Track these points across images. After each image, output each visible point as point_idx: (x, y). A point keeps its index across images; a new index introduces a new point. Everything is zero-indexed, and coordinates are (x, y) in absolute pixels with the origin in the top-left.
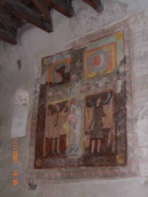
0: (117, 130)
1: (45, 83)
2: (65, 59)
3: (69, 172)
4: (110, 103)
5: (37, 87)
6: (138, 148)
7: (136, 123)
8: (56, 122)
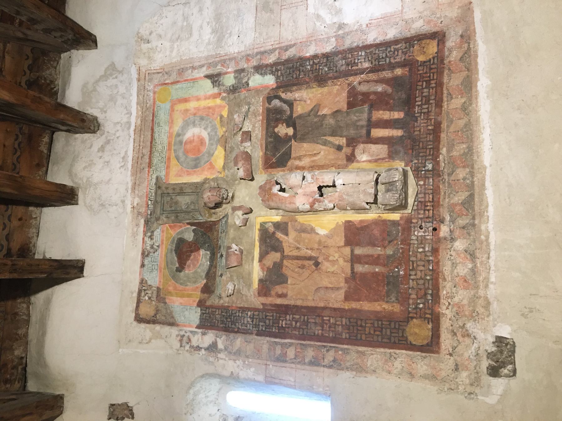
0: (357, 70)
1: (199, 310)
2: (162, 243)
3: (451, 211)
4: (292, 98)
5: (201, 346)
6: (404, 11)
7: (347, 24)
8: (306, 263)
